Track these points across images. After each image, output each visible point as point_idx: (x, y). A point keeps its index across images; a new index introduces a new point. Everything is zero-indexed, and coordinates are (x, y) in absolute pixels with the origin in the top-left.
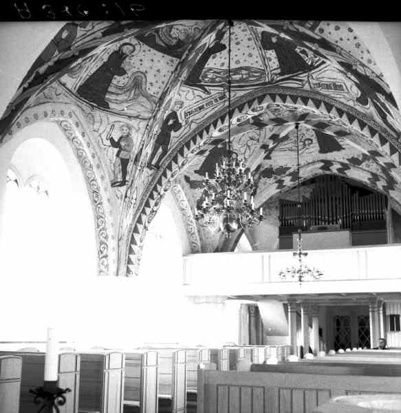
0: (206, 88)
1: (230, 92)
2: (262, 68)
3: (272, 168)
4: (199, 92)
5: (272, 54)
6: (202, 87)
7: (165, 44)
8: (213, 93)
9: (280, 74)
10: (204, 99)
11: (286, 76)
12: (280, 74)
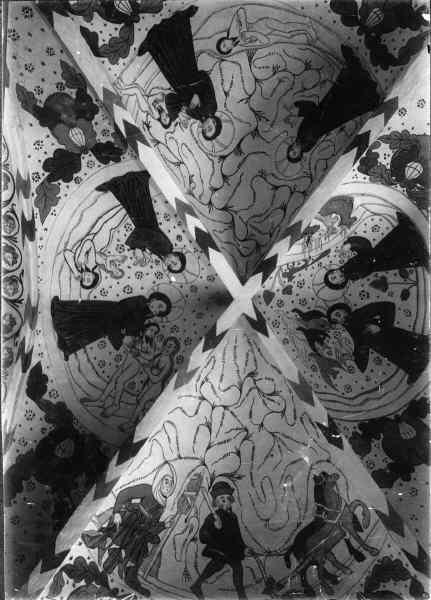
3: (68, 180)
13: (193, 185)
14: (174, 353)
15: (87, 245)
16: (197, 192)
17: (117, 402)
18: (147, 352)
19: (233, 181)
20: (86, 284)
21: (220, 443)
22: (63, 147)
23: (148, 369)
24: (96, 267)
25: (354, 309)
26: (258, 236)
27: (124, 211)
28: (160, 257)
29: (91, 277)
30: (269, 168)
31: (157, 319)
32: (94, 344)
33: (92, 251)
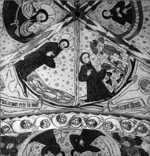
0: (27, 89)
1: (42, 105)
2: (73, 95)
4: (20, 88)
5: (84, 85)
6: (25, 86)
7: (20, 34)
8: (30, 97)
9: (86, 101)
10: (21, 99)
11: (90, 103)
12: (86, 101)
25: (73, 148)
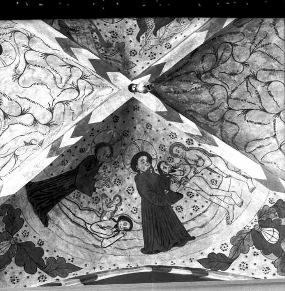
13: (33, 142)
14: (184, 147)
15: (94, 227)
16: (41, 138)
17: (229, 194)
18: (184, 171)
19: (26, 105)
20: (128, 226)
21: (261, 102)
22: (13, 259)
23: (199, 169)
24: (114, 220)
26: (74, 79)
27: (64, 201)
28: (101, 165)
29: (121, 223)
30: (10, 71)
31: (154, 164)
32: (179, 215)
33: (99, 223)
